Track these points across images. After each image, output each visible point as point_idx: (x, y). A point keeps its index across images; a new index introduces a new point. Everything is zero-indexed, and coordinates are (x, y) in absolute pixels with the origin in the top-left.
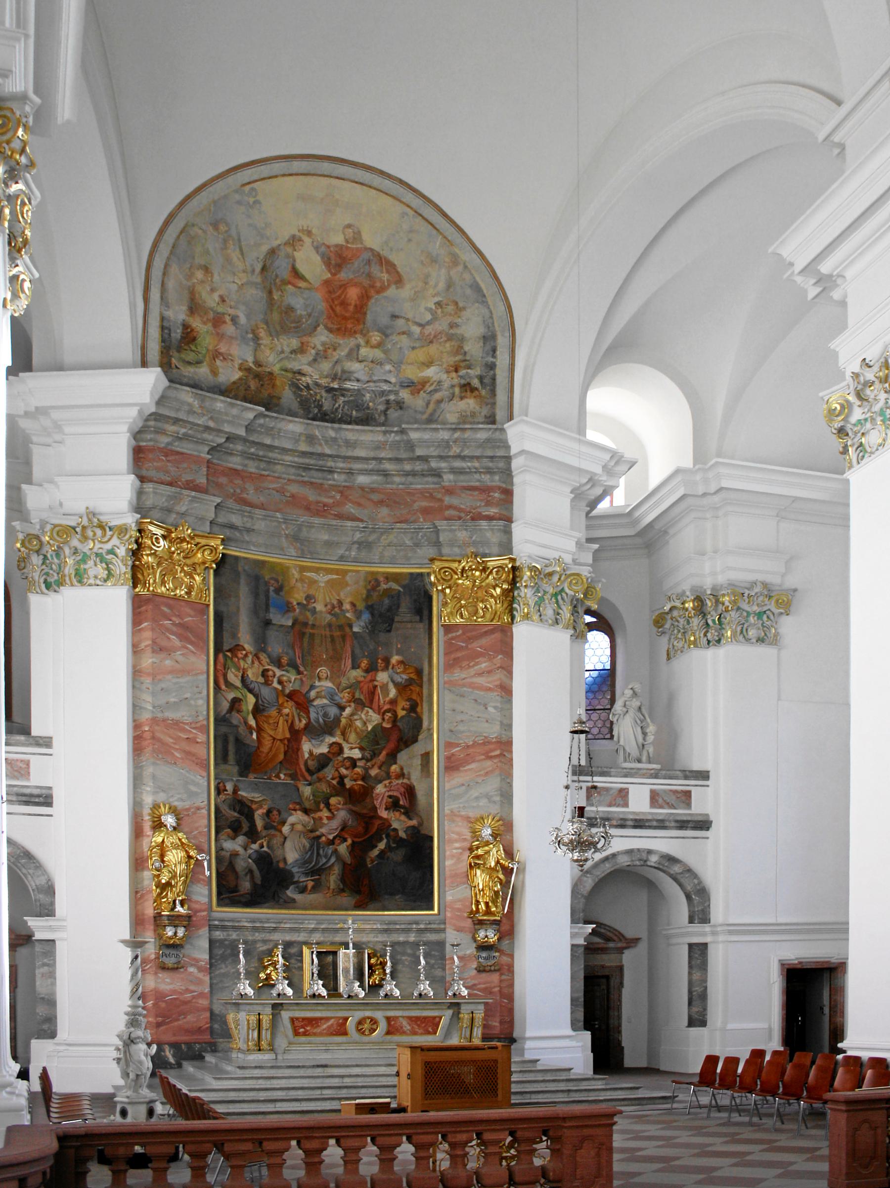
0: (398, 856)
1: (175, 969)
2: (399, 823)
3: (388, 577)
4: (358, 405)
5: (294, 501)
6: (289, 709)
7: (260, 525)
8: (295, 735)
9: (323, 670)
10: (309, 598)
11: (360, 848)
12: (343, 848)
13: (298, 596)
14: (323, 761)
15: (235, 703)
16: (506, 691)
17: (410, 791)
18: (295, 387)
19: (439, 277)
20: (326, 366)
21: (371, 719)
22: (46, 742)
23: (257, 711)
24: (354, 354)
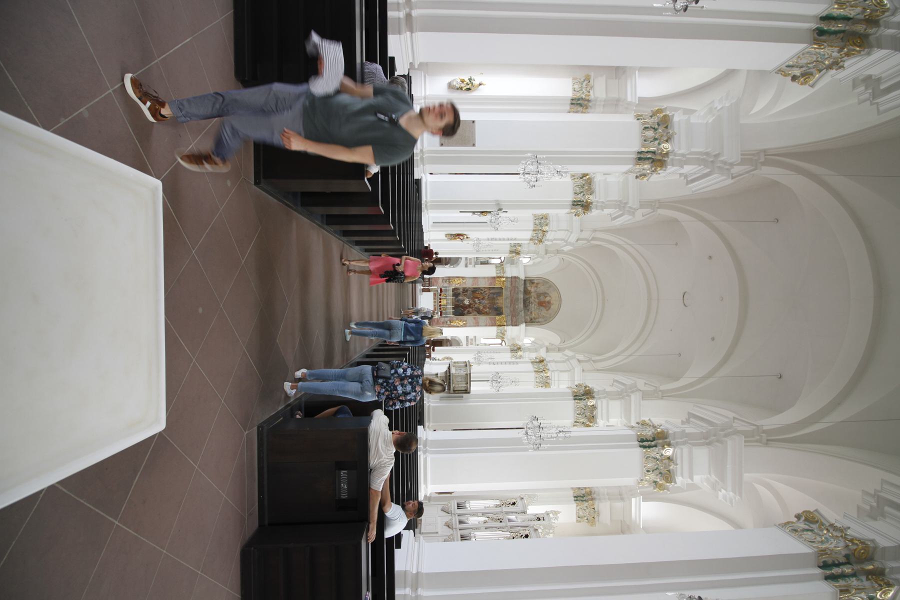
0: (461, 312)
1: (443, 282)
2: (466, 312)
3: (503, 310)
4: (528, 306)
5: (513, 297)
6: (482, 297)
7: (508, 293)
8: (478, 298)
9: (488, 302)
10: (498, 300)
11: (462, 307)
12: (462, 304)
13: (498, 298)
14: (475, 302)
15: (482, 290)
16: (486, 326)
17: (471, 313)
18: (529, 297)
19: (547, 316)
20: (533, 301)
21: (481, 308)
22: (474, 266)
23: (481, 293)
24: (535, 305)
